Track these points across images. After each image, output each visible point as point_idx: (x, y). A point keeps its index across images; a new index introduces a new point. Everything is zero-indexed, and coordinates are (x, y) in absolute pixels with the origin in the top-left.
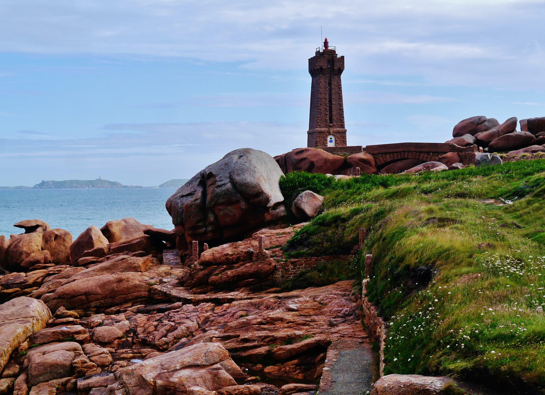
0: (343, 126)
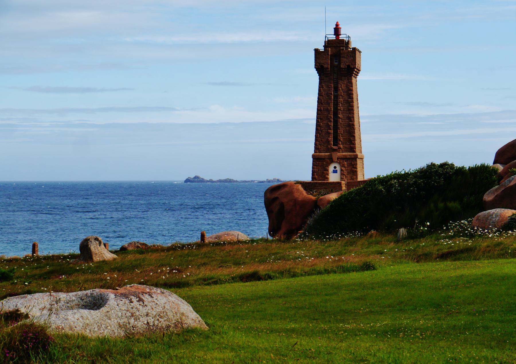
0: (352, 149)
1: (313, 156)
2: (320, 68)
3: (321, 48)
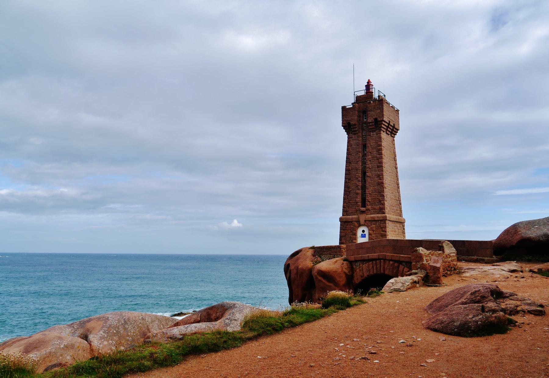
0: (382, 210)
1: (341, 219)
2: (347, 126)
3: (349, 105)
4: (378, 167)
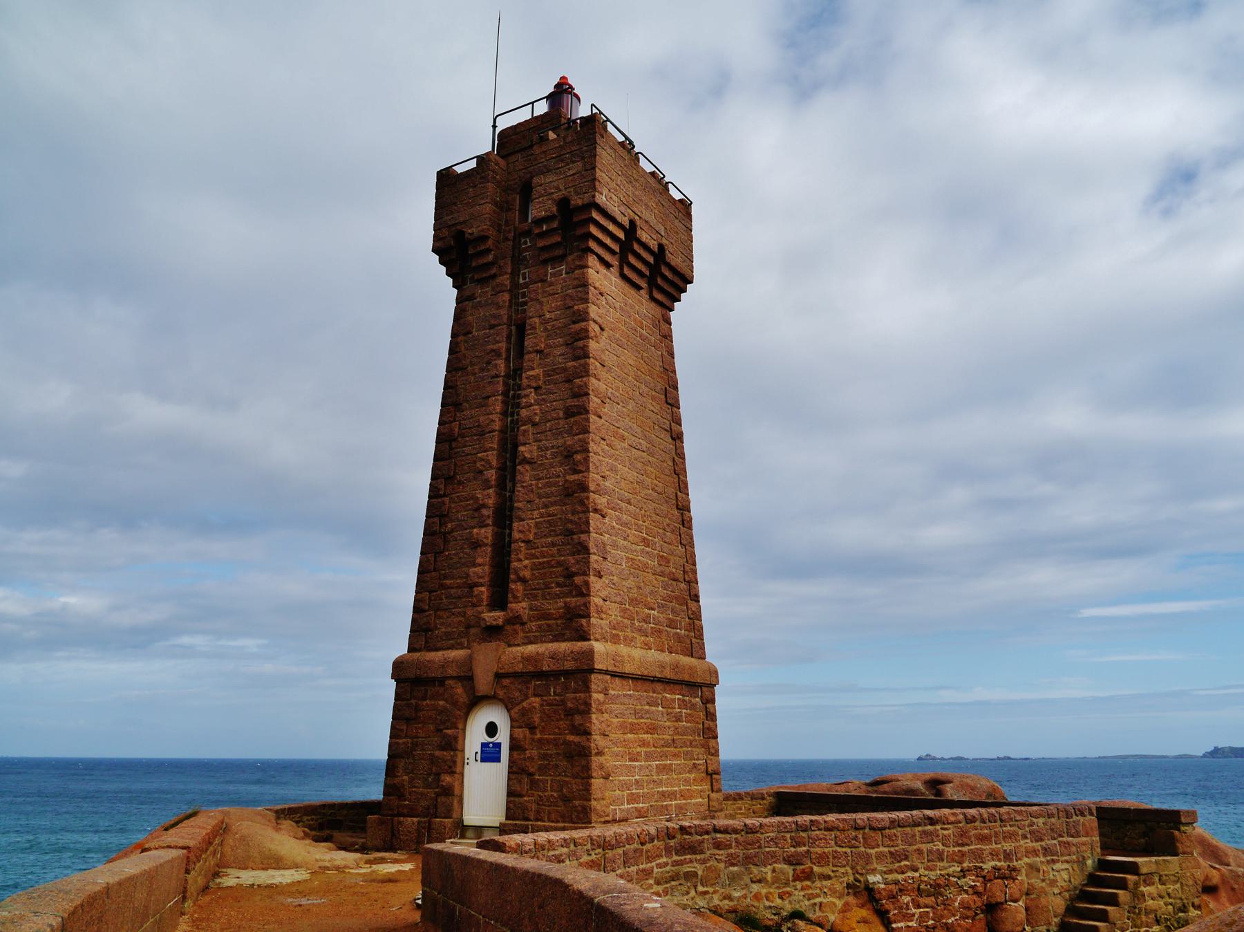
0: (574, 623)
4: (569, 413)
